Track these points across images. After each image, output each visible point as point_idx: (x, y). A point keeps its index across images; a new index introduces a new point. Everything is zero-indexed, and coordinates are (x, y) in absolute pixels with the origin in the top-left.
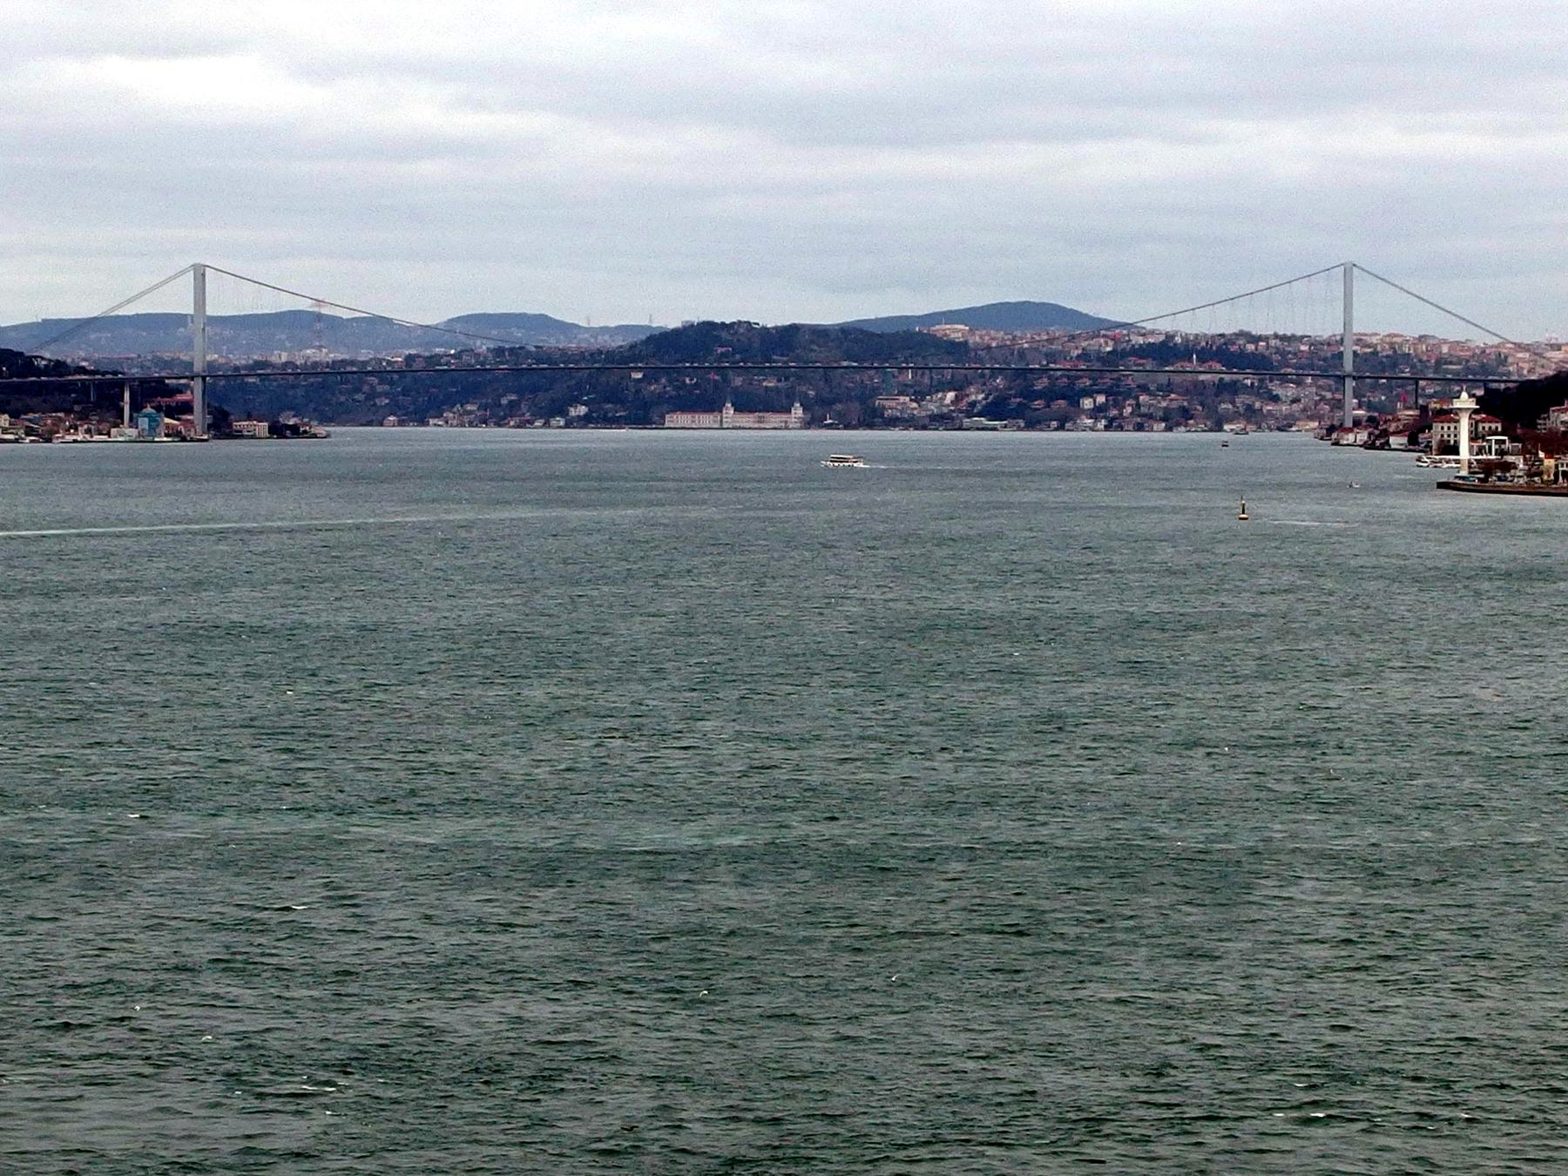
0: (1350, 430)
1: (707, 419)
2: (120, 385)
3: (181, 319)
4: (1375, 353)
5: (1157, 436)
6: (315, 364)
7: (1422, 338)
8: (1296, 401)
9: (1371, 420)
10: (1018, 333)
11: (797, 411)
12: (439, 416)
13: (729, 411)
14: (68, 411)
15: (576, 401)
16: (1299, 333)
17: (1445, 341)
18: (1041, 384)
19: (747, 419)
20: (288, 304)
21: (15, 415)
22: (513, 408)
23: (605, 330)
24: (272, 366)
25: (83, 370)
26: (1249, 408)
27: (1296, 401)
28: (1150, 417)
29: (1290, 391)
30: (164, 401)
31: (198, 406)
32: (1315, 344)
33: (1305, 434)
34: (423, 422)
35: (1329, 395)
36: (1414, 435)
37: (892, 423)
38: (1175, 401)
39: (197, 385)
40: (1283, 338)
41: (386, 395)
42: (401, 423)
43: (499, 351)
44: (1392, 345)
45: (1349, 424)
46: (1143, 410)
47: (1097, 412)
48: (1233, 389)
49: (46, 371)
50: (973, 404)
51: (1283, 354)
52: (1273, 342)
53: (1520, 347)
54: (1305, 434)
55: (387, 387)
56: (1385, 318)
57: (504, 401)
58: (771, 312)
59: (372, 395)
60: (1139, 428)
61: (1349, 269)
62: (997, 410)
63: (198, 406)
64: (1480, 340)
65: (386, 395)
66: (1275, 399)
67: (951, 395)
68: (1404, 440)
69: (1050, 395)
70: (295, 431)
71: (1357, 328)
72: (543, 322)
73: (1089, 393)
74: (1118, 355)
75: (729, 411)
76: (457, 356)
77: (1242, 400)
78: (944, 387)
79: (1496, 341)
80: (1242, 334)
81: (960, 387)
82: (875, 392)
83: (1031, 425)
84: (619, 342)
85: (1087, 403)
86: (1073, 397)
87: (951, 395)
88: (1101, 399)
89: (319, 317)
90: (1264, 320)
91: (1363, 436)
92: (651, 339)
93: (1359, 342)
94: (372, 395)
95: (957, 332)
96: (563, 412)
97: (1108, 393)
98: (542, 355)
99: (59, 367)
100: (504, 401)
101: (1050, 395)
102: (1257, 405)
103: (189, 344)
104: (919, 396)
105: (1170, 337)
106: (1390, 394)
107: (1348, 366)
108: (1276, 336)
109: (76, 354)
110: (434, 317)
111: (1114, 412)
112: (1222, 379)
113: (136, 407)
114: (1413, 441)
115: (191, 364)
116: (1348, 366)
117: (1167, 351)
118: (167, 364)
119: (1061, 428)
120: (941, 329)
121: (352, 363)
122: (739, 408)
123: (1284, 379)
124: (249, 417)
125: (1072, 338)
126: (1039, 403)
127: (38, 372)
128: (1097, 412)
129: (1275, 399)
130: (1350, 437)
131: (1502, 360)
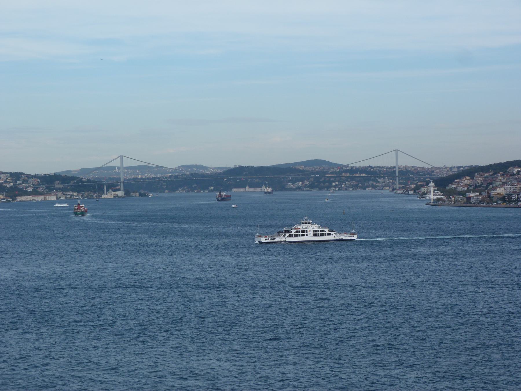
0: (399, 190)
1: (241, 190)
2: (103, 185)
3: (114, 168)
4: (402, 170)
5: (351, 192)
6: (148, 178)
7: (413, 167)
8: (384, 182)
9: (403, 187)
10: (316, 167)
12: (178, 190)
13: (247, 187)
14: (91, 191)
16: (383, 166)
17: (418, 167)
18: (322, 179)
19: (252, 190)
20: (138, 164)
21: (78, 192)
22: (195, 188)
23: (215, 168)
25: (94, 181)
27: (384, 182)
28: (349, 187)
29: (381, 180)
30: (114, 188)
31: (122, 189)
32: (387, 168)
33: (387, 191)
34: (174, 191)
35: (391, 181)
36: (415, 190)
37: (286, 190)
38: (354, 183)
39: (122, 184)
40: (380, 167)
41: (165, 185)
42: (169, 192)
43: (192, 174)
44: (406, 168)
45: (398, 188)
46: (347, 185)
47: (336, 186)
48: (369, 179)
49: (85, 182)
50: (306, 185)
51: (380, 171)
52: (377, 168)
53: (437, 168)
54: (387, 191)
56: (405, 162)
57: (193, 186)
58: (257, 163)
59: (162, 185)
60: (346, 190)
61: (397, 151)
62: (312, 186)
63: (122, 189)
64: (427, 166)
65: (165, 185)
66: (379, 182)
67: (301, 183)
68: (412, 192)
69: (324, 182)
70: (145, 195)
71: (400, 164)
73: (334, 182)
74: (340, 173)
75: (247, 187)
76: (182, 175)
77: (371, 183)
79: (430, 167)
80: (370, 167)
81: (302, 180)
83: (321, 189)
84: (219, 171)
85: (333, 184)
86: (330, 182)
87: (301, 183)
88: (337, 183)
89: (149, 167)
90: (375, 163)
91: (402, 191)
92: (228, 171)
93: (399, 169)
94: (162, 185)
95: (302, 167)
96: (208, 189)
98: (203, 175)
99: (89, 181)
100: (193, 186)
101: (324, 182)
102: (374, 184)
103: (119, 174)
104: (293, 184)
105: (352, 167)
106: (412, 179)
107: (397, 174)
108: (378, 167)
109: (91, 177)
110: (175, 166)
112: (366, 177)
113: (107, 191)
114: (415, 192)
115: (120, 178)
116: (397, 174)
117: (353, 170)
118: (113, 179)
119: (327, 190)
120: (298, 167)
121: (157, 178)
122: (250, 187)
123: (381, 178)
124: (134, 192)
125: (330, 169)
126: (322, 184)
127: (83, 182)
128: (336, 186)
129: (379, 182)
130: (399, 192)
131: (433, 171)
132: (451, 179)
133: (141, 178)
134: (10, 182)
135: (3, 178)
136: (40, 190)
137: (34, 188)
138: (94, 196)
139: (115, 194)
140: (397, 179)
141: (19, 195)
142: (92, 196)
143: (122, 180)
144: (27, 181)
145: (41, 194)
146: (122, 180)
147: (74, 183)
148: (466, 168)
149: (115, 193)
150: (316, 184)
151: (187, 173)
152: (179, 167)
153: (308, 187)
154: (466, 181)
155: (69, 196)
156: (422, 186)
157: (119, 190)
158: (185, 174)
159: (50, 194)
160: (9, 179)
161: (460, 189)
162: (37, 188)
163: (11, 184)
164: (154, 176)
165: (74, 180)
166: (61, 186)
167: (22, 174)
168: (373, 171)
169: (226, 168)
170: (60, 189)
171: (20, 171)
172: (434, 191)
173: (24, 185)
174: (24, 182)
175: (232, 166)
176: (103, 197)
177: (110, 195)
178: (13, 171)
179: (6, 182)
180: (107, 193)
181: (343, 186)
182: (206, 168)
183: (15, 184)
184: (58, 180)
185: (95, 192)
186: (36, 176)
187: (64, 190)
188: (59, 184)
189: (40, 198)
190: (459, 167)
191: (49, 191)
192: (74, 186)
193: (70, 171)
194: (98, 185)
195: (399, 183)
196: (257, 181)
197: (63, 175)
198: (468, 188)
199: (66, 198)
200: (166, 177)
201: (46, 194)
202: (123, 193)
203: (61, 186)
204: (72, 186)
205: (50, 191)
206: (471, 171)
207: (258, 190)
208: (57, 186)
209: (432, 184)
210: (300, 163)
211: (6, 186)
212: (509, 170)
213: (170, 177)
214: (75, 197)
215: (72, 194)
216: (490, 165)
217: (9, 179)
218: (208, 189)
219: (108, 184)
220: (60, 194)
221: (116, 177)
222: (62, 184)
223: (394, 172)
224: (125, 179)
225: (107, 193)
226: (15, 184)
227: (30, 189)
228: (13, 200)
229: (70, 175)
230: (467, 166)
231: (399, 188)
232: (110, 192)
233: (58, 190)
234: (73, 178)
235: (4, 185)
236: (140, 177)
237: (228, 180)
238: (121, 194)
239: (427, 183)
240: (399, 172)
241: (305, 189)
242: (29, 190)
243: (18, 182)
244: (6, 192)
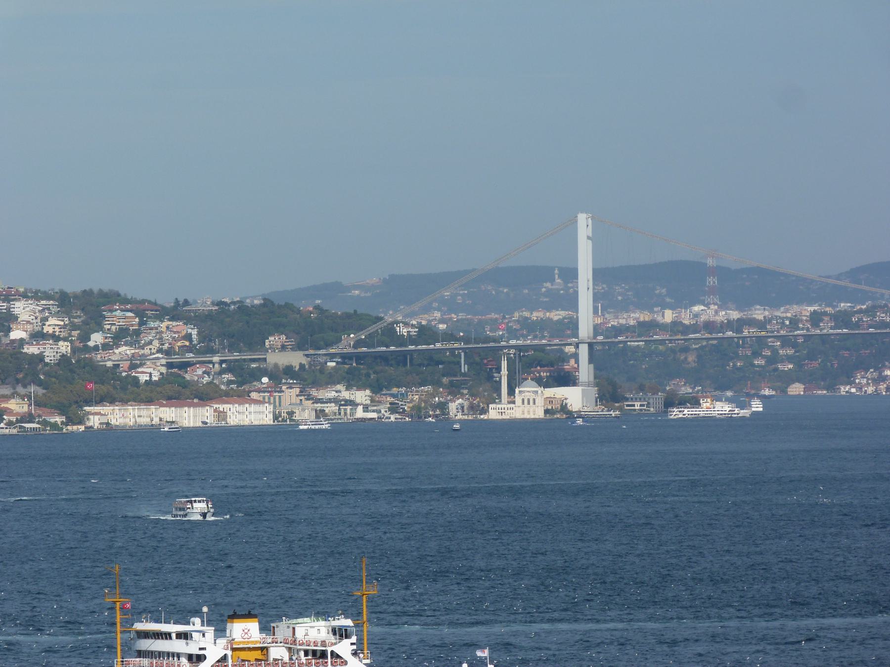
2: (496, 353)
6: (709, 326)
14: (437, 383)
21: (377, 388)
24: (663, 327)
25: (449, 336)
31: (585, 371)
39: (584, 350)
41: (790, 359)
49: (412, 340)
55: (790, 352)
59: (774, 359)
65: (790, 359)
99: (426, 334)
115: (573, 325)
121: (751, 322)
127: (401, 341)
133: (676, 327)
134: (56, 338)
135: (24, 316)
136: (196, 375)
137: (169, 365)
138: (453, 407)
139: (550, 400)
141: (100, 401)
142: (443, 406)
143: (585, 330)
144: (137, 333)
145: (204, 396)
147: (358, 343)
149: (550, 392)
155: (331, 408)
157: (567, 379)
159: (242, 397)
160: (53, 324)
162: (185, 366)
163: (64, 347)
164: (735, 315)
166: (296, 359)
167: (111, 298)
170: (289, 371)
171: (106, 288)
173: (125, 350)
174: (120, 336)
176: (493, 413)
177: (528, 403)
178: (74, 287)
179: (38, 336)
180: (511, 392)
183: (82, 348)
184: (279, 328)
185: (454, 390)
186: (177, 312)
187: (308, 379)
188: (283, 348)
189: (190, 417)
191: (240, 384)
192: (359, 358)
193: (335, 289)
194: (468, 353)
197: (306, 306)
199: (320, 414)
200: (795, 322)
201: (227, 396)
202: (593, 392)
203: (296, 359)
204: (346, 358)
205: (244, 381)
211: (40, 358)
213: (816, 319)
214: (360, 413)
215: (346, 395)
217: (53, 324)
219: (518, 348)
220: (290, 395)
221: (557, 315)
222: (299, 347)
224: (597, 329)
225: (511, 392)
226: (82, 348)
227: (151, 372)
228: (70, 421)
229: (337, 309)
232: (528, 390)
233: (281, 375)
234: (353, 321)
235: (32, 350)
236: (669, 316)
238: (574, 397)
242: (143, 378)
243: (97, 339)
244: (40, 384)
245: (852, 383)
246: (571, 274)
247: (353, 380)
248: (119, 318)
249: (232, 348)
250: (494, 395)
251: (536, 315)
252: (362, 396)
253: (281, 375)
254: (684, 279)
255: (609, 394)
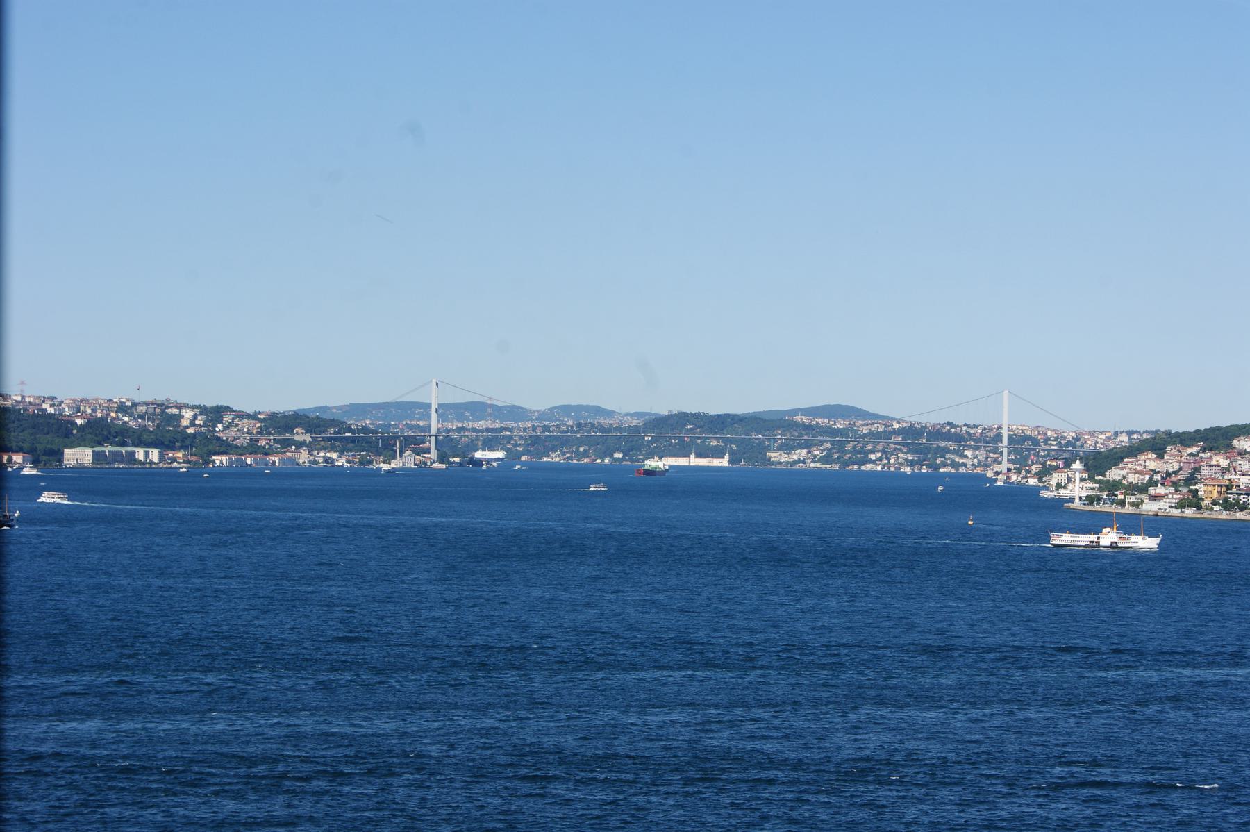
1: (683, 462)
6: (488, 430)
11: (727, 457)
13: (693, 456)
15: (618, 450)
20: (468, 398)
22: (585, 454)
26: (953, 461)
39: (433, 439)
48: (944, 452)
49: (359, 431)
51: (968, 433)
72: (598, 410)
73: (872, 452)
75: (693, 456)
78: (801, 447)
80: (949, 423)
81: (808, 446)
82: (768, 449)
84: (634, 422)
85: (872, 457)
87: (805, 451)
88: (879, 455)
90: (961, 417)
97: (883, 452)
99: (365, 429)
105: (912, 425)
111: (885, 462)
115: (430, 426)
117: (912, 432)
120: (798, 418)
122: (698, 455)
123: (969, 447)
127: (353, 432)
129: (966, 457)
132: (1115, 457)
140: (1005, 451)
143: (433, 431)
146: (433, 431)
147: (335, 433)
148: (1145, 436)
150: (836, 456)
151: (570, 423)
152: (552, 409)
153: (819, 461)
154: (1148, 463)
156: (1057, 468)
158: (564, 424)
161: (1133, 478)
164: (497, 425)
165: (335, 427)
166: (308, 438)
167: (228, 409)
168: (956, 434)
169: (649, 414)
172: (1082, 480)
175: (664, 412)
178: (210, 403)
181: (892, 461)
182: (611, 414)
186: (253, 417)
187: (310, 447)
190: (1130, 433)
193: (326, 408)
195: (1009, 461)
196: (714, 443)
197: (312, 415)
198: (1151, 478)
200: (525, 429)
203: (308, 438)
206: (1158, 444)
207: (716, 462)
208: (298, 438)
209: (1077, 465)
210: (805, 411)
212: (1235, 443)
213: (534, 428)
216: (1197, 431)
218: (611, 456)
221: (422, 423)
223: (999, 437)
230: (1146, 432)
231: (1009, 470)
233: (299, 445)
234: (333, 423)
237: (654, 440)
239: (1068, 465)
240: (1010, 436)
241: (812, 465)
245: (548, 456)
246: (429, 406)
247: (332, 449)
248: (228, 418)
249: (279, 433)
250: (394, 458)
251: (414, 422)
252: (334, 455)
253: (299, 445)
254: (478, 409)
255: (442, 458)
